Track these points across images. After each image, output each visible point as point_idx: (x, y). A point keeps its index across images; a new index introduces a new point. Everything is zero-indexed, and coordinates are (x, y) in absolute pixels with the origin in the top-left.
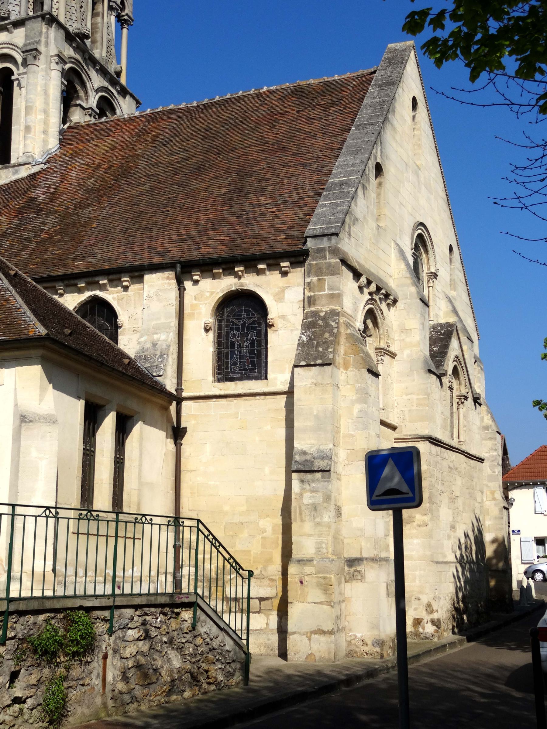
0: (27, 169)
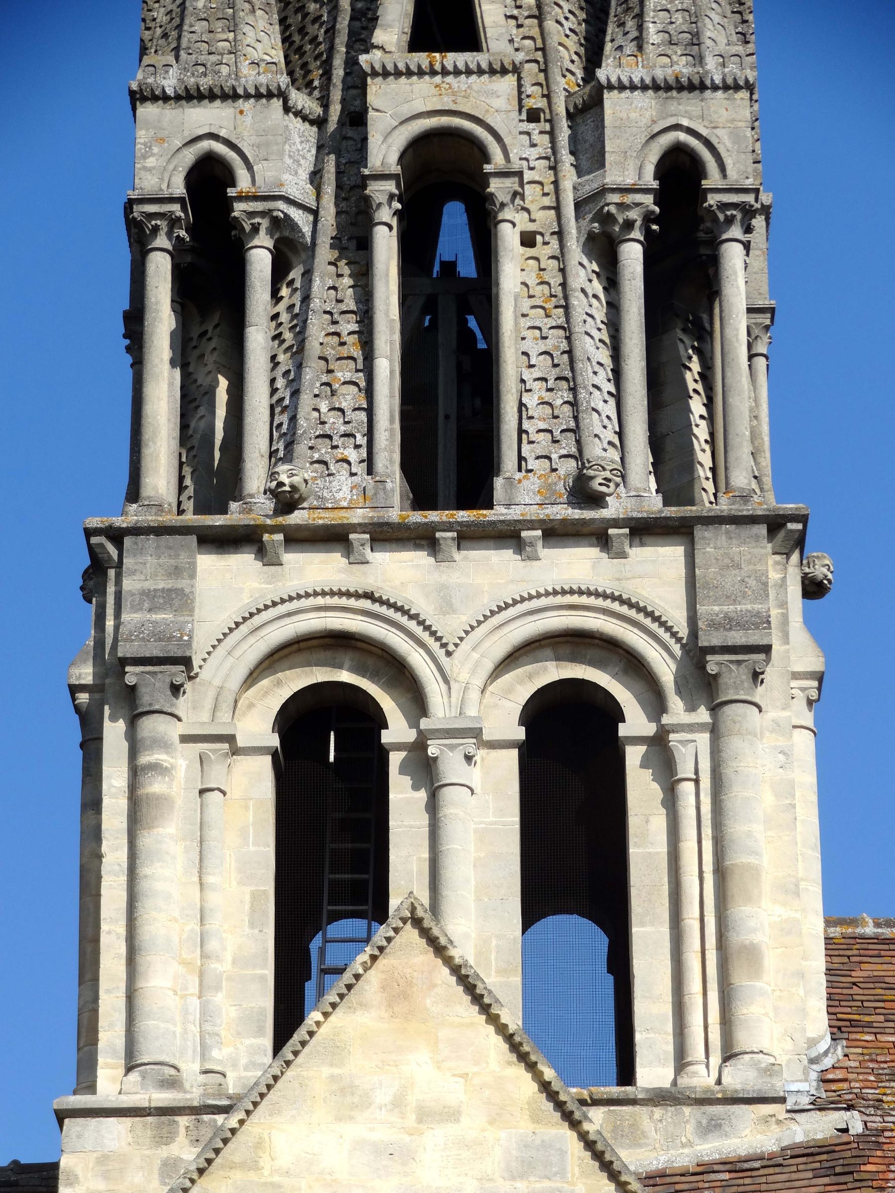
0: (766, 1120)
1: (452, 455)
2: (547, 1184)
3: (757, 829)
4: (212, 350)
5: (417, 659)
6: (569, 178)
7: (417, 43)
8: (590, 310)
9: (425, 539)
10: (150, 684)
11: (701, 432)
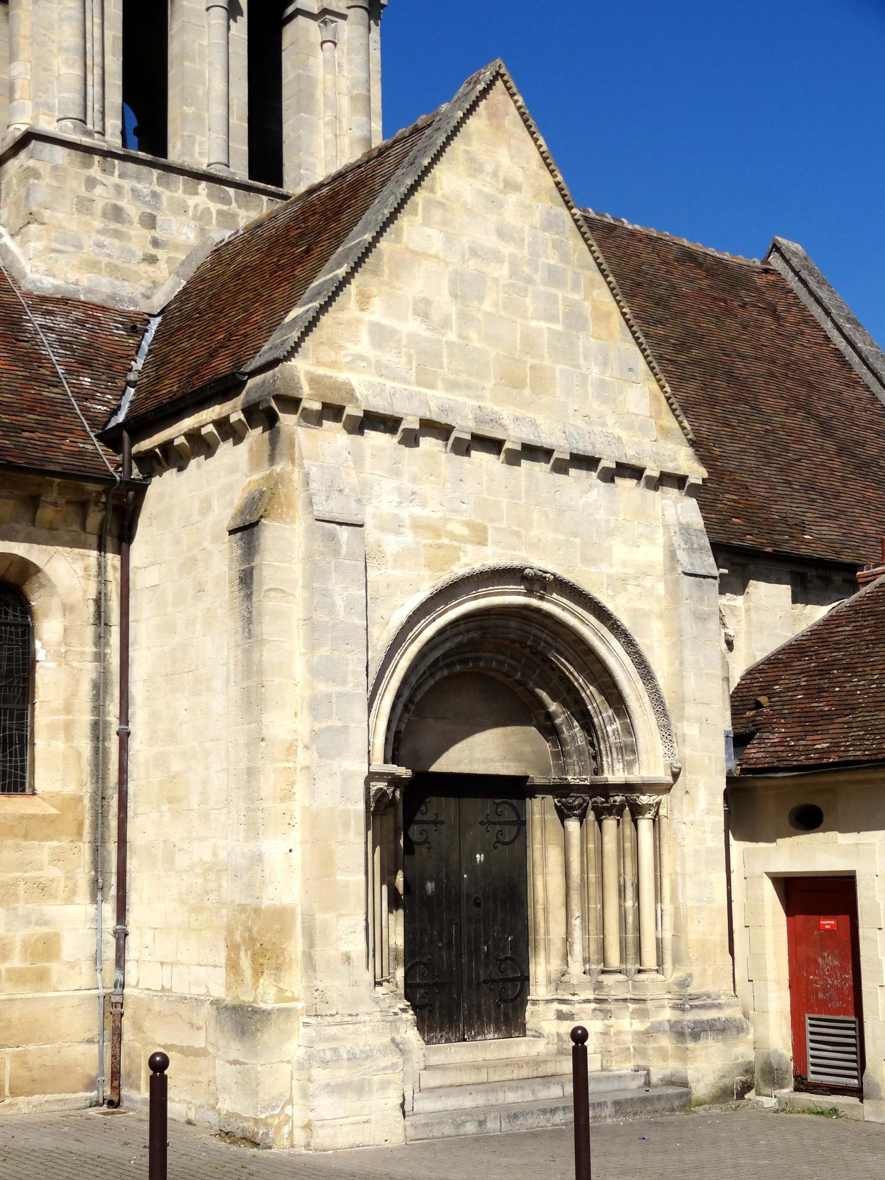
2: (557, 237)
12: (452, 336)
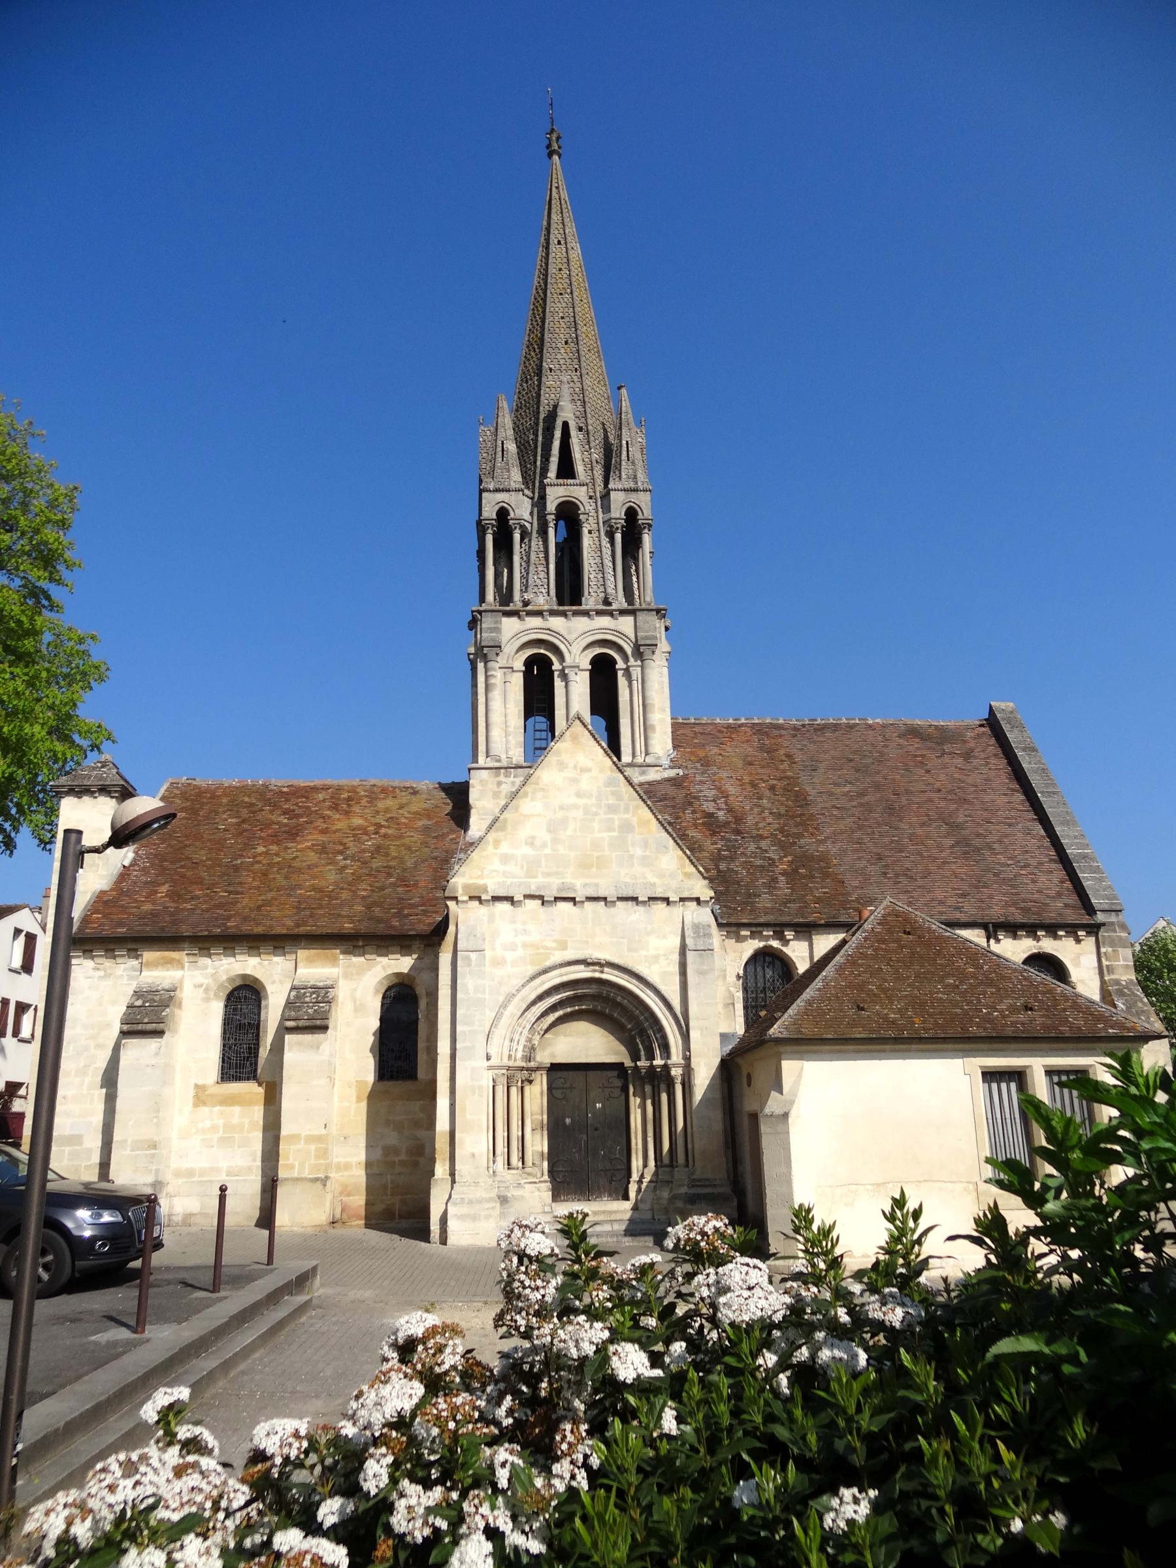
1: (570, 591)
3: (654, 694)
4: (503, 561)
5: (562, 647)
6: (601, 515)
7: (558, 477)
8: (607, 552)
9: (564, 614)
10: (491, 655)
11: (636, 585)
12: (548, 851)
